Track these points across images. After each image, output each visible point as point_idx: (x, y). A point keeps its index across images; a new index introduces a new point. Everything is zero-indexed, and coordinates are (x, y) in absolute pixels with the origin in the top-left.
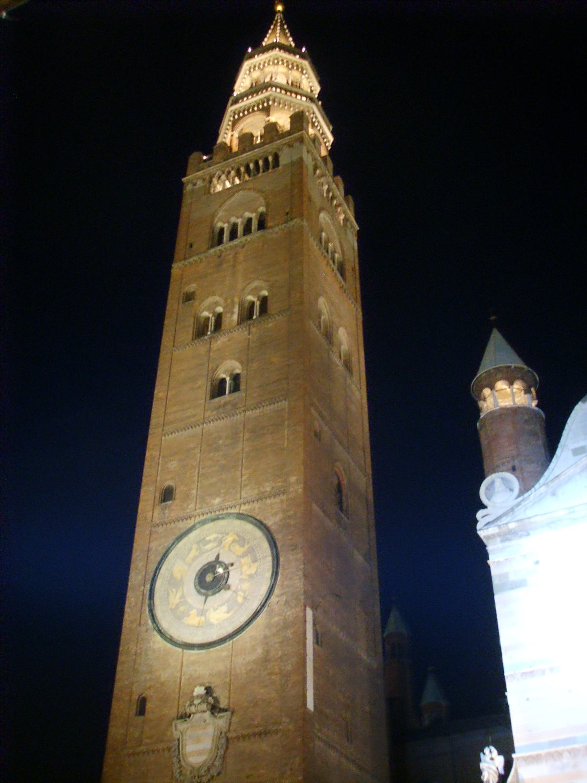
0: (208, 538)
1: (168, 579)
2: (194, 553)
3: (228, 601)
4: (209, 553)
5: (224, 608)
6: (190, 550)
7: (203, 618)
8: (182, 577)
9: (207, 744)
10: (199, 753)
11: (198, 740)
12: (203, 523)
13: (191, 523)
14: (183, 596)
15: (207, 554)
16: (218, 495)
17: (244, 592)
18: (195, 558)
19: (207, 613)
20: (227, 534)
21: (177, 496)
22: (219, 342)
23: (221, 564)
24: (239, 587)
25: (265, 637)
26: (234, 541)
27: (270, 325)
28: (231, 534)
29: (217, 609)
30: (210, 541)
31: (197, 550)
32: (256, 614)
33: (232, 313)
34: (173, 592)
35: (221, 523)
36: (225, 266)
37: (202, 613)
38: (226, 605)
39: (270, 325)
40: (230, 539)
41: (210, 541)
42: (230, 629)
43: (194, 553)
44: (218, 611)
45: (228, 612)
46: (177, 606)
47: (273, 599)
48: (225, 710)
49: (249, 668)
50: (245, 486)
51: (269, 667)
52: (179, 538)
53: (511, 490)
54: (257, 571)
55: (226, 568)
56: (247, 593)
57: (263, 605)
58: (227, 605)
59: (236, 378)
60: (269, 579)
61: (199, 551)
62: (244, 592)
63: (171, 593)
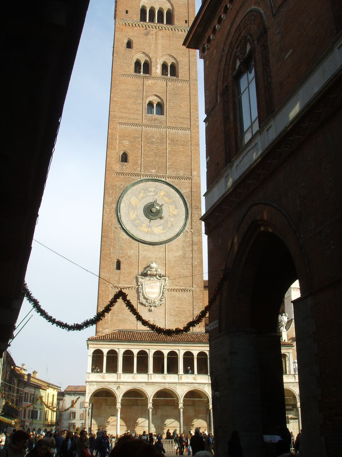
0: (150, 189)
1: (128, 204)
2: (142, 195)
3: (163, 224)
4: (151, 197)
5: (161, 227)
6: (140, 193)
7: (149, 229)
8: (136, 205)
10: (153, 293)
11: (152, 287)
14: (137, 215)
15: (150, 197)
16: (154, 168)
17: (172, 222)
18: (143, 198)
19: (152, 227)
20: (161, 190)
21: (130, 161)
23: (158, 204)
24: (169, 219)
25: (183, 246)
26: (164, 195)
27: (179, 85)
28: (162, 191)
29: (158, 227)
30: (151, 191)
31: (144, 194)
32: (178, 235)
33: (156, 68)
34: (131, 212)
36: (150, 36)
38: (162, 226)
39: (179, 85)
40: (162, 193)
41: (151, 191)
43: (142, 195)
44: (158, 228)
46: (135, 220)
49: (176, 259)
50: (169, 168)
51: (186, 261)
52: (134, 184)
54: (178, 214)
55: (161, 206)
56: (173, 223)
57: (181, 231)
58: (163, 226)
60: (184, 219)
61: (145, 195)
62: (172, 222)
63: (130, 211)
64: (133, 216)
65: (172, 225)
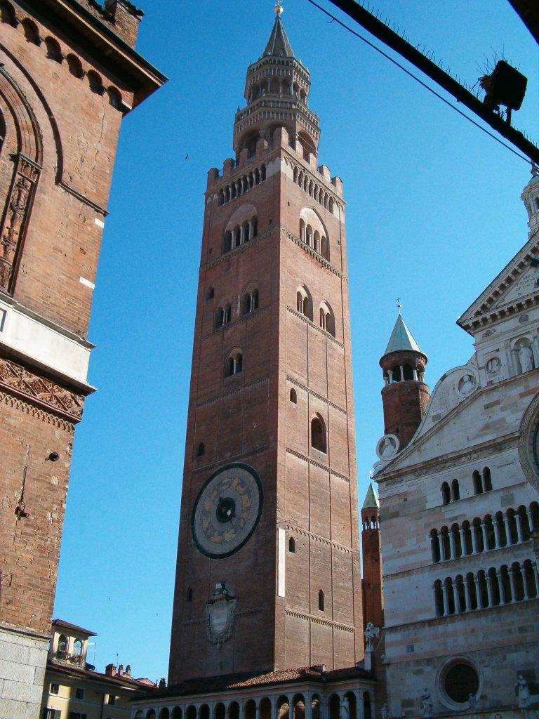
9: (224, 619)
10: (219, 624)
12: (221, 471)
13: (214, 471)
14: (210, 523)
22: (229, 332)
33: (237, 308)
35: (231, 470)
36: (231, 269)
37: (221, 534)
40: (236, 482)
42: (236, 544)
45: (235, 533)
47: (260, 524)
48: (233, 598)
53: (395, 447)
59: (240, 358)
64: (206, 525)
65: (245, 523)
